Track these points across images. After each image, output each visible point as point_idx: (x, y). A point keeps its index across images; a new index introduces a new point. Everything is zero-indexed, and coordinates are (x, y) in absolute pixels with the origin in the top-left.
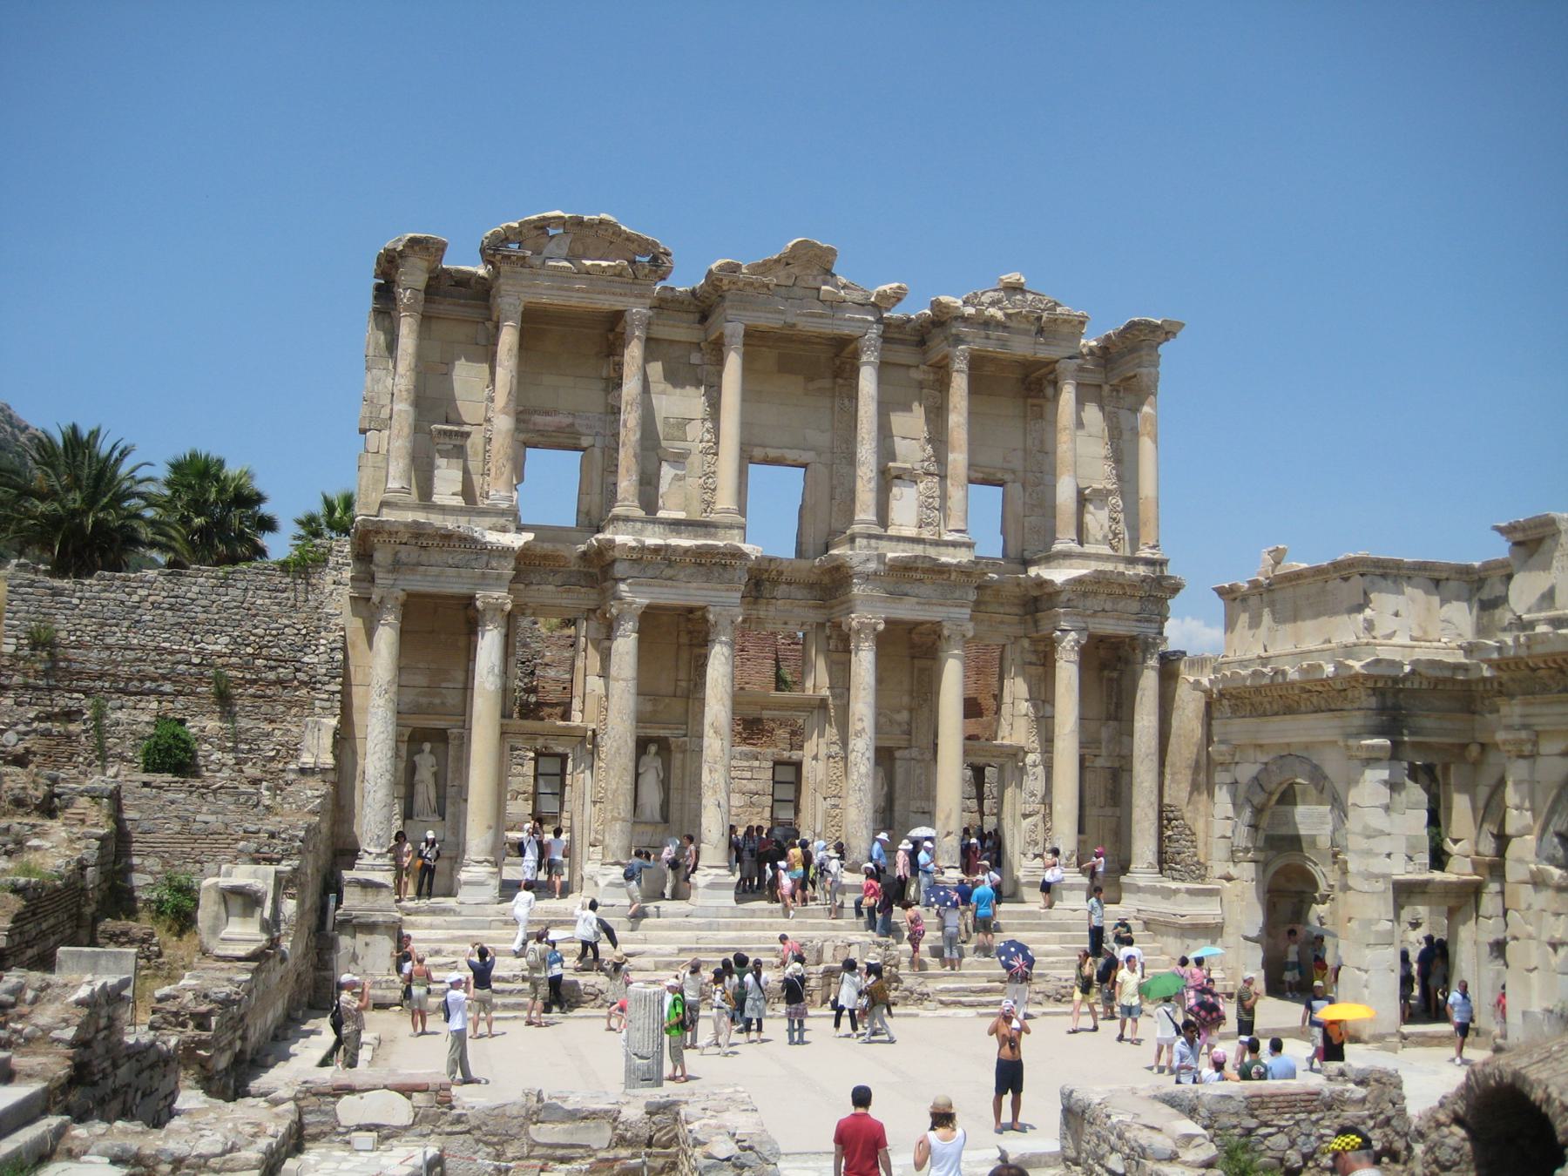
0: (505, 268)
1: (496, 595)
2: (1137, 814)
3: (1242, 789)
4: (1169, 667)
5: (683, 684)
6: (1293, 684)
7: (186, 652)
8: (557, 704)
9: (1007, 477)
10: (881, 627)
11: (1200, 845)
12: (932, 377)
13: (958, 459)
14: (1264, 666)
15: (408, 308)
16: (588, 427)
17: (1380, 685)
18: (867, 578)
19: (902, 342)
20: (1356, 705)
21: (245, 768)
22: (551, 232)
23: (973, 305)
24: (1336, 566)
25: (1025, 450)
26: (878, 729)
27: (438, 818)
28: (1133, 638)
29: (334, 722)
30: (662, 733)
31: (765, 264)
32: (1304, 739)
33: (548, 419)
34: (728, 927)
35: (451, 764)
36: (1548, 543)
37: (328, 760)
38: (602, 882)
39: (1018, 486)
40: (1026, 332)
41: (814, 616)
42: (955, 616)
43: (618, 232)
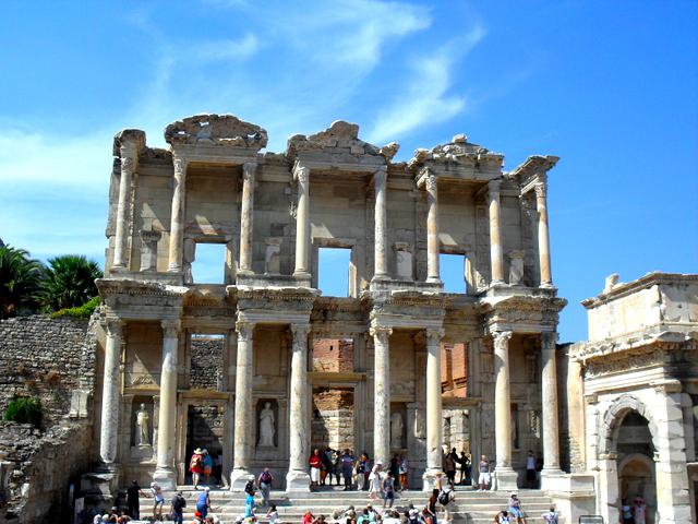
3: (602, 416)
4: (561, 351)
5: (284, 369)
6: (623, 352)
9: (466, 249)
10: (391, 332)
11: (582, 453)
12: (421, 196)
17: (672, 348)
18: (382, 305)
19: (403, 177)
22: (202, 124)
28: (539, 335)
34: (304, 503)
37: (84, 412)
40: (469, 166)
41: (358, 329)
42: (434, 325)
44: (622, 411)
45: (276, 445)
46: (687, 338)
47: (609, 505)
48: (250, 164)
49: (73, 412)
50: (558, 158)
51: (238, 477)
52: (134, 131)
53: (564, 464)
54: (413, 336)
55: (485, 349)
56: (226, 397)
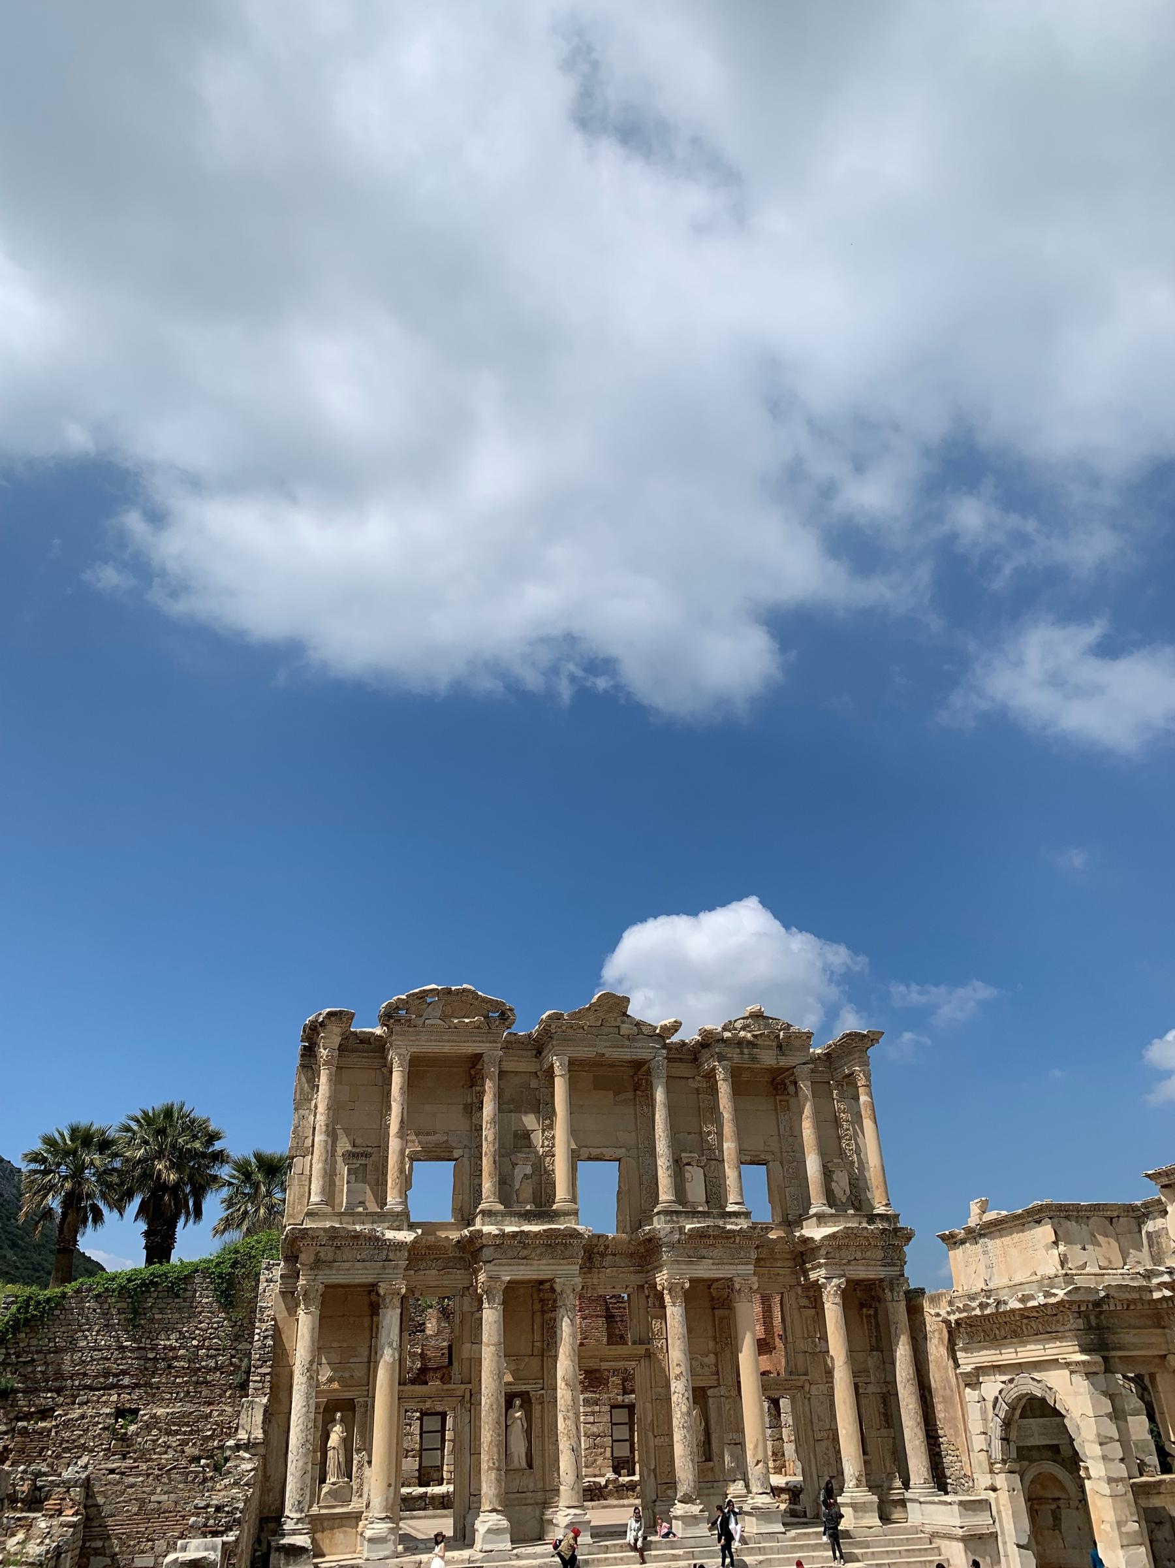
2: (908, 1434)
3: (990, 1405)
5: (538, 1344)
6: (1013, 1311)
7: (144, 1348)
8: (437, 1369)
9: (769, 1157)
10: (687, 1285)
11: (964, 1458)
14: (988, 1298)
17: (1083, 1309)
18: (672, 1246)
19: (681, 1060)
20: (1067, 1328)
21: (186, 1449)
22: (429, 1000)
26: (693, 1372)
28: (881, 1280)
29: (265, 1400)
30: (524, 1388)
31: (580, 1012)
37: (259, 1434)
40: (769, 1048)
41: (637, 1279)
42: (742, 1272)
44: (1020, 1398)
45: (530, 1466)
46: (1102, 1294)
47: (1019, 1546)
48: (491, 1051)
49: (242, 1435)
51: (487, 1526)
52: (341, 1012)
53: (939, 1479)
54: (709, 1287)
55: (805, 1302)
56: (459, 1393)
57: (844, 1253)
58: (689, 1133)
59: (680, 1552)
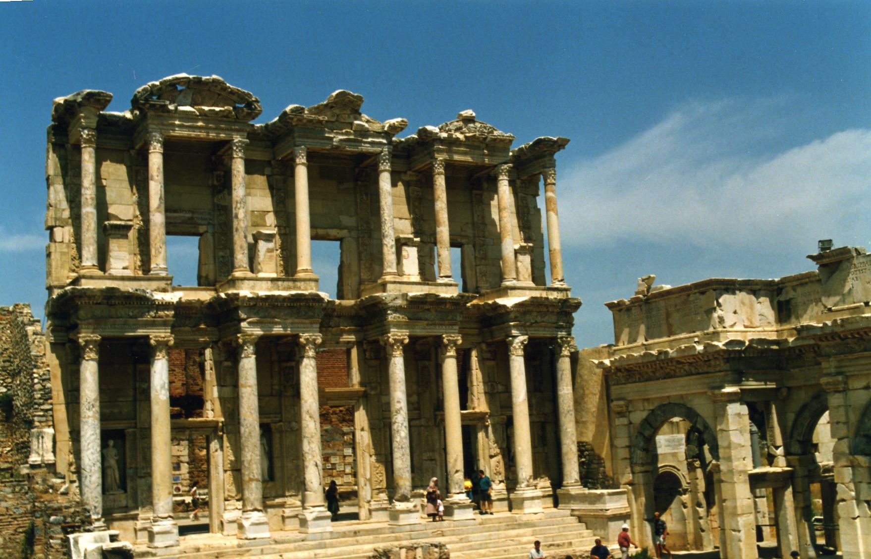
0: (151, 113)
1: (163, 335)
5: (276, 387)
6: (672, 359)
9: (464, 241)
10: (407, 341)
13: (444, 232)
15: (88, 141)
16: (202, 219)
18: (397, 309)
20: (717, 369)
22: (179, 88)
23: (447, 132)
24: (697, 286)
25: (473, 224)
27: (122, 492)
30: (265, 421)
31: (318, 108)
32: (681, 393)
33: (175, 215)
35: (128, 453)
36: (845, 265)
38: (246, 524)
39: (471, 246)
43: (225, 89)
49: (34, 458)
50: (567, 141)
52: (99, 94)
55: (488, 355)
57: (528, 317)
58: (400, 219)
59: (401, 534)
